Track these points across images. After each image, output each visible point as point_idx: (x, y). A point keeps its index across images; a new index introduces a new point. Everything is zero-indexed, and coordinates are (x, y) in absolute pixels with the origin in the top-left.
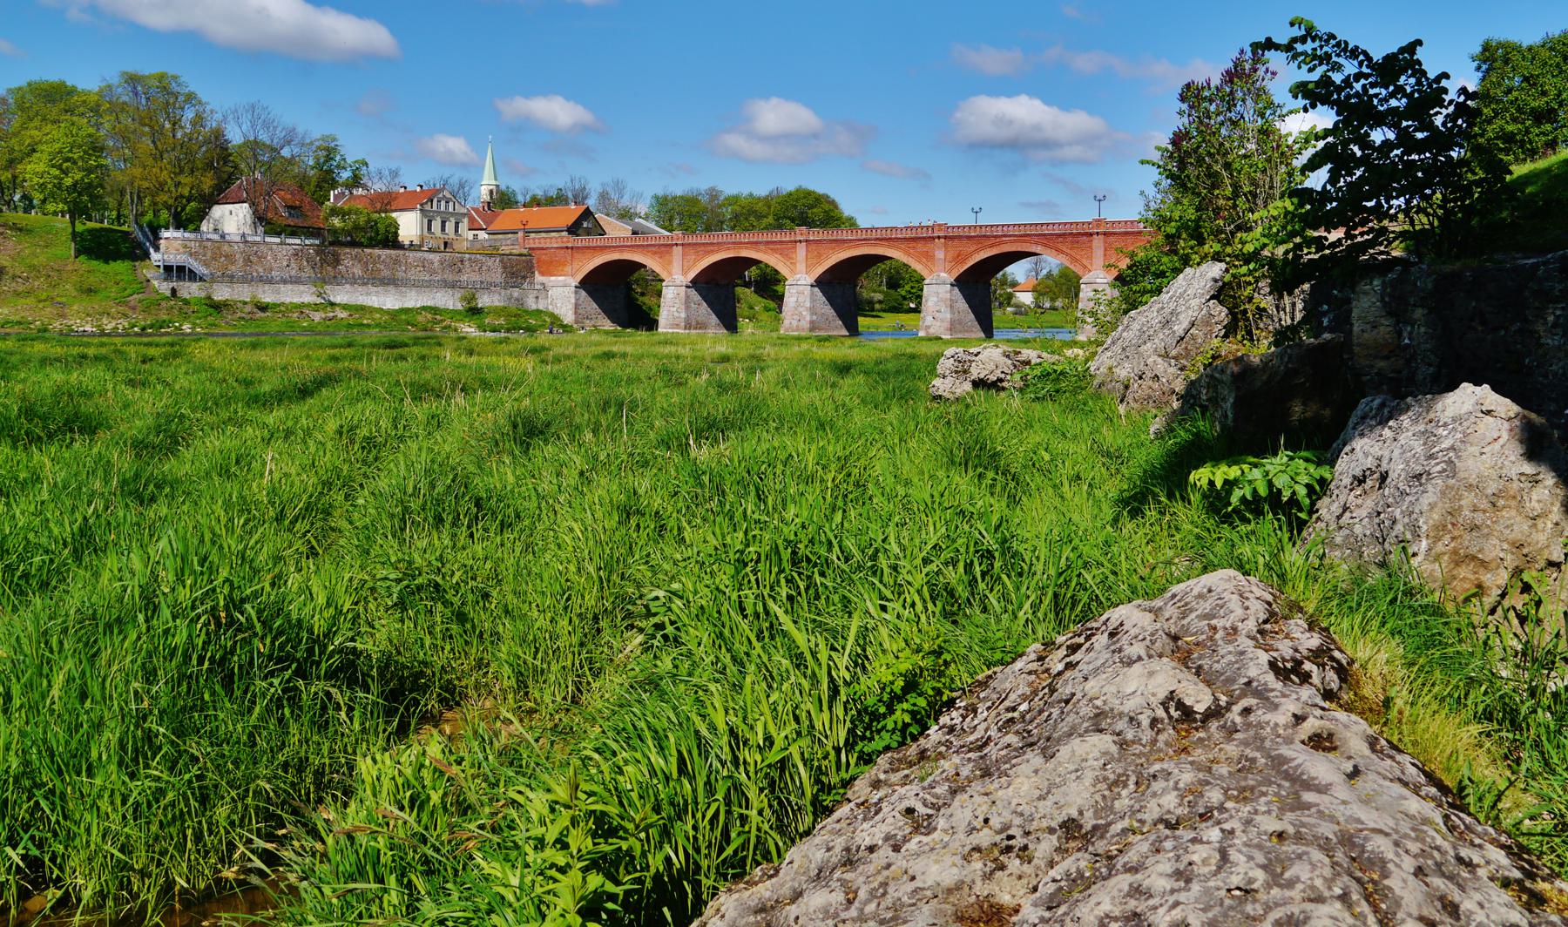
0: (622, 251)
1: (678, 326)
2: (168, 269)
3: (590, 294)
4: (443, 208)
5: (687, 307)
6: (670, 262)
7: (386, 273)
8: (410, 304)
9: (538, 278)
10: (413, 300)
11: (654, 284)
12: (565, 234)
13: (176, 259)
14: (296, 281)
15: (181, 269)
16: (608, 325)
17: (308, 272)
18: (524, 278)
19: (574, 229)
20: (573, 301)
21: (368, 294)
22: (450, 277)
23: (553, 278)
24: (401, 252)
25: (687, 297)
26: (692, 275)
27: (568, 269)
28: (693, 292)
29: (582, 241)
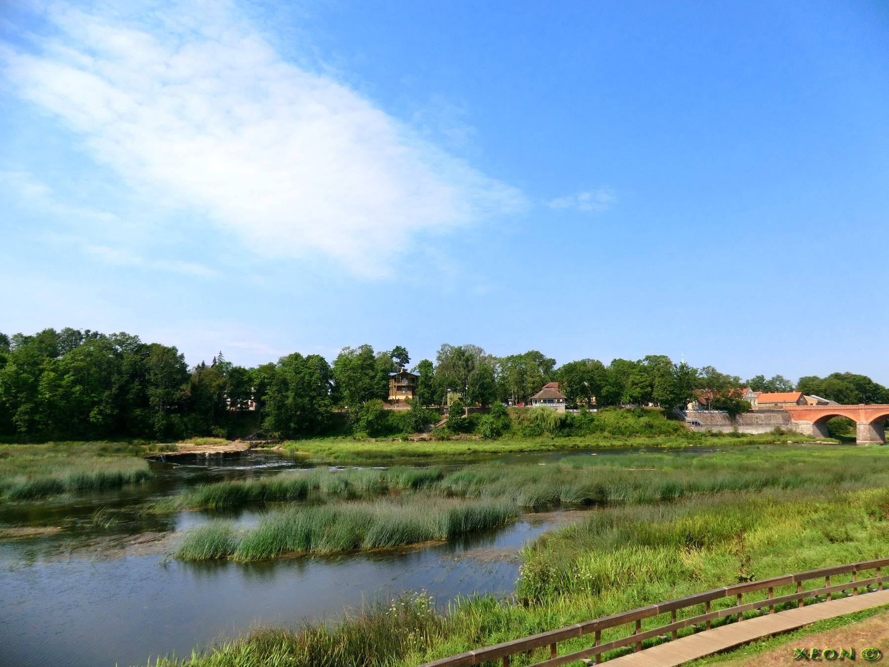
0: (834, 411)
1: (867, 440)
2: (693, 423)
3: (817, 426)
4: (750, 396)
5: (870, 434)
6: (859, 416)
7: (749, 422)
8: (760, 432)
9: (793, 421)
10: (761, 431)
11: (852, 423)
12: (795, 404)
13: (694, 420)
14: (725, 425)
15: (696, 422)
16: (823, 438)
17: (727, 422)
18: (789, 421)
19: (798, 403)
20: (812, 430)
21: (748, 429)
22: (768, 422)
23: (800, 421)
24: (752, 414)
25: (869, 429)
26: (871, 420)
27: (807, 418)
28: (871, 427)
29: (801, 408)
